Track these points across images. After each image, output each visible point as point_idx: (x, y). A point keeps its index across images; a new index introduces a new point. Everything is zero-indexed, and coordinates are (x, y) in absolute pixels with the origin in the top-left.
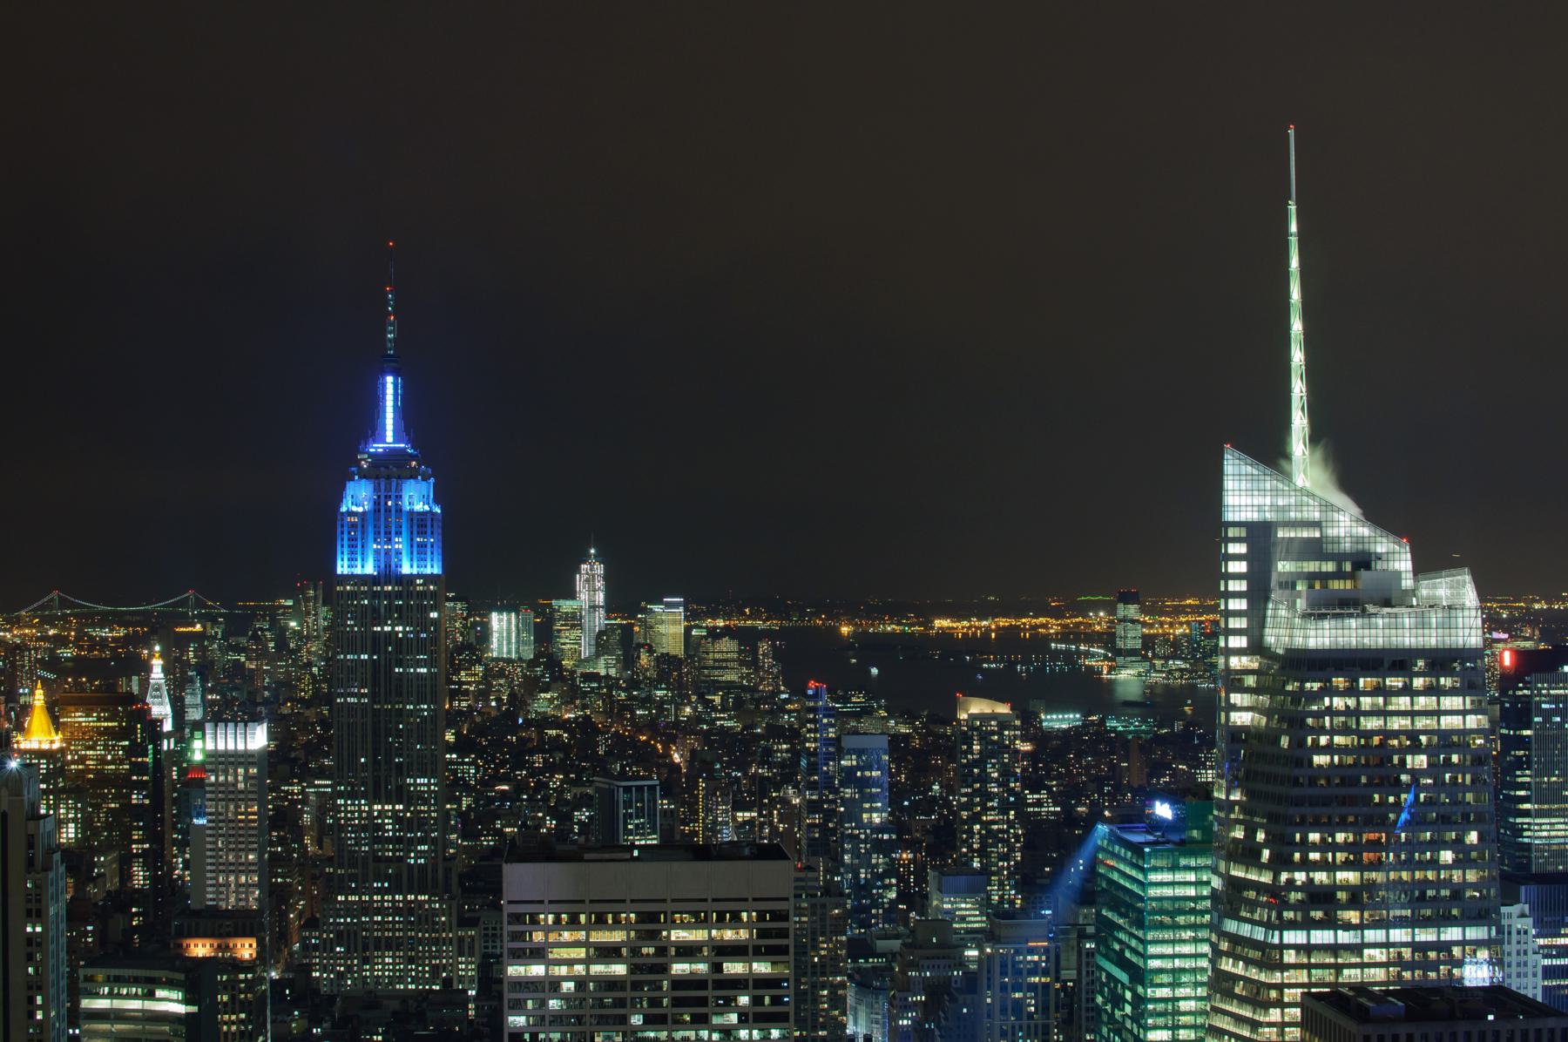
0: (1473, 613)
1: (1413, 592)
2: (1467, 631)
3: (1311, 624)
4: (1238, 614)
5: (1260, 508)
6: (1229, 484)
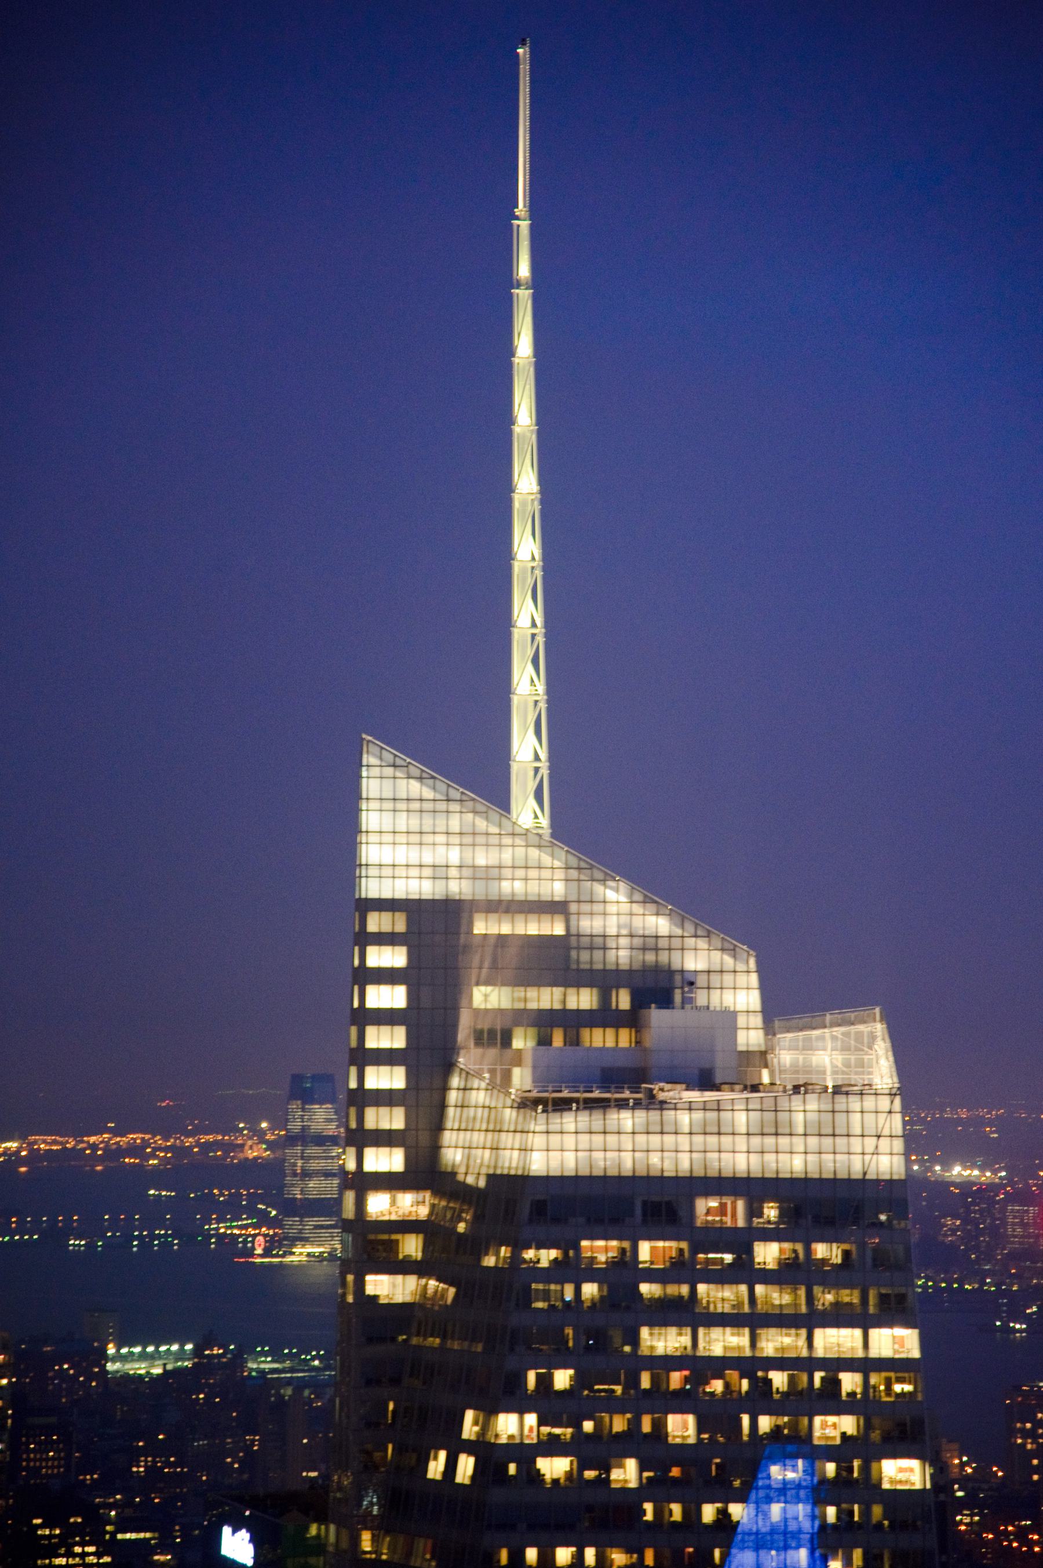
0: (884, 1103)
1: (762, 1057)
2: (870, 1143)
3: (538, 1122)
4: (385, 1098)
5: (440, 873)
6: (371, 818)
